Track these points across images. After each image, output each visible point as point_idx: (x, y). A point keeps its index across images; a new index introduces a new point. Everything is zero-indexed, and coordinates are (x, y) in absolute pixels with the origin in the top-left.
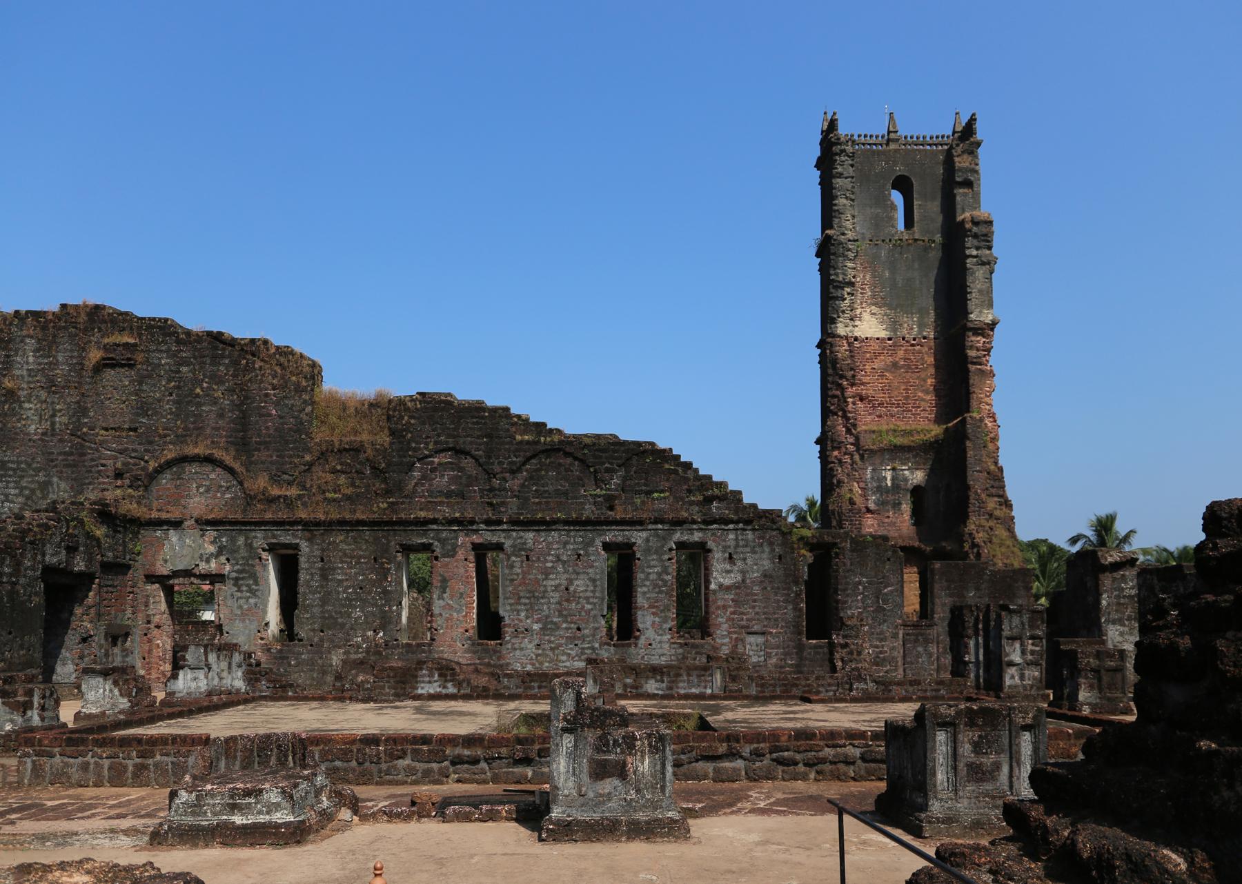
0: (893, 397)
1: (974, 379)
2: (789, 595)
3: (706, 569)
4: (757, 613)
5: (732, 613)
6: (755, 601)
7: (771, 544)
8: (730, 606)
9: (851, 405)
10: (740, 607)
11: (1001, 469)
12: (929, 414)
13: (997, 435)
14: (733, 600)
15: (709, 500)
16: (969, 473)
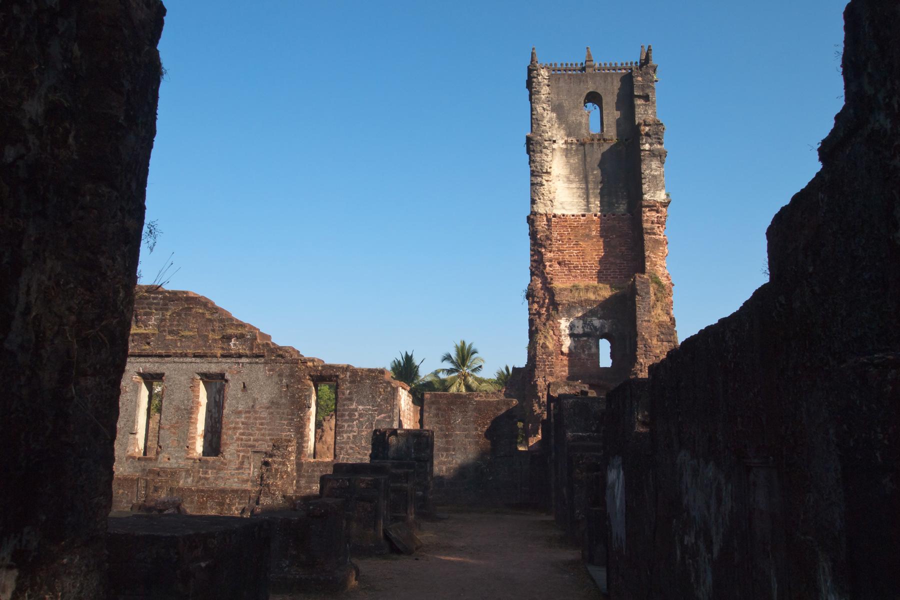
0: (587, 261)
1: (648, 244)
2: (292, 419)
3: (223, 397)
4: (263, 435)
5: (243, 434)
6: (262, 424)
7: (280, 375)
8: (239, 428)
9: (548, 268)
10: (248, 430)
11: (673, 320)
12: (619, 275)
13: (671, 291)
14: (243, 423)
15: (228, 338)
16: (639, 322)
